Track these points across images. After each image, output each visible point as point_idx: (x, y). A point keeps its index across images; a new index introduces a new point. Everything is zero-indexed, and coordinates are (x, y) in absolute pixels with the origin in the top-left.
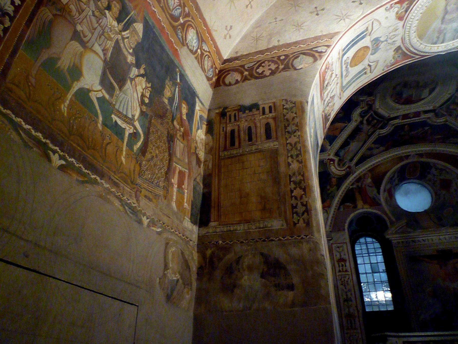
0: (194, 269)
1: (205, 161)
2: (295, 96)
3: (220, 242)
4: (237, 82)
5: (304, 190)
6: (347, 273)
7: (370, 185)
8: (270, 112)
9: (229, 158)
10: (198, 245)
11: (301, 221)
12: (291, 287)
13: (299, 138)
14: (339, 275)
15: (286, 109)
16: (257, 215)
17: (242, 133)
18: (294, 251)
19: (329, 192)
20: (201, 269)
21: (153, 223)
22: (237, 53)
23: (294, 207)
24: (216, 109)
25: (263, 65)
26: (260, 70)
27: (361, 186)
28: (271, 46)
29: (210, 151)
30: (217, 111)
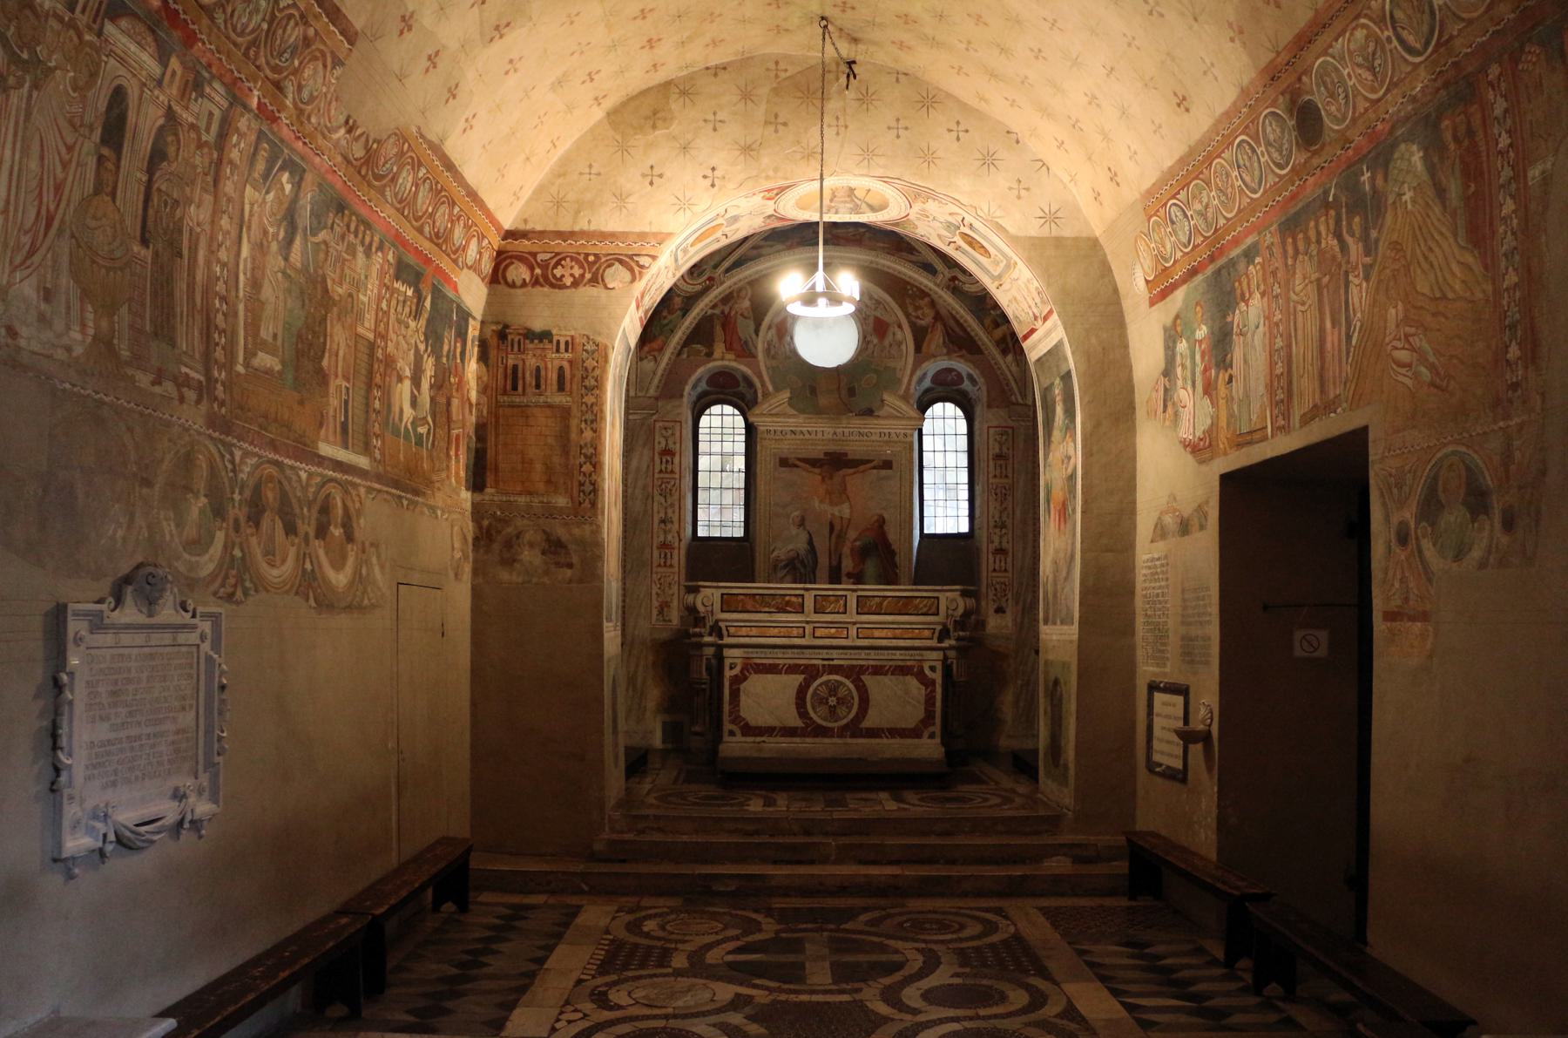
0: (470, 540)
1: (478, 404)
2: (600, 334)
3: (499, 513)
4: (524, 284)
5: (594, 467)
6: (673, 476)
7: (746, 314)
8: (567, 350)
9: (509, 406)
10: (472, 513)
11: (587, 501)
12: (570, 566)
13: (596, 398)
14: (658, 479)
15: (586, 351)
16: (541, 486)
17: (528, 375)
18: (576, 531)
19: (666, 322)
20: (476, 539)
21: (443, 511)
22: (526, 221)
23: (581, 484)
24: (492, 323)
25: (563, 262)
26: (558, 272)
27: (729, 313)
28: (577, 228)
29: (483, 390)
30: (494, 328)
